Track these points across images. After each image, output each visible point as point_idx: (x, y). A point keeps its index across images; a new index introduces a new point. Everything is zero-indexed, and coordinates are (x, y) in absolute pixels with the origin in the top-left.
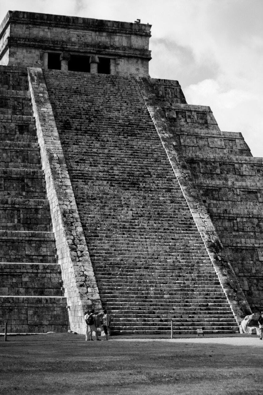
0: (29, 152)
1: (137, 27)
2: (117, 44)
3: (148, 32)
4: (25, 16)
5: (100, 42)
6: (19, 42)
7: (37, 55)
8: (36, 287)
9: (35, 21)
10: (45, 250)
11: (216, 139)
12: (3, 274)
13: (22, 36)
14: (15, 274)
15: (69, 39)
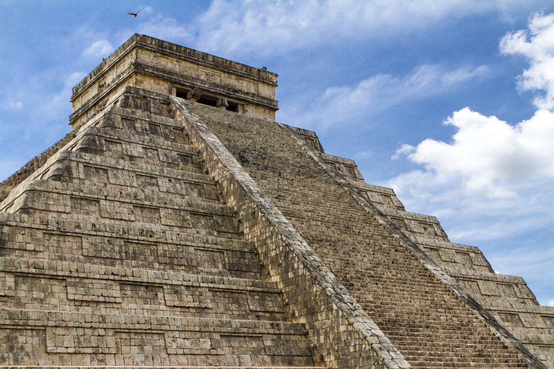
0: (205, 185)
1: (262, 74)
2: (246, 91)
3: (275, 81)
4: (154, 43)
5: (229, 84)
6: (146, 70)
7: (166, 89)
8: (283, 354)
9: (164, 50)
10: (270, 304)
11: (374, 193)
12: (239, 335)
13: (150, 64)
14: (254, 335)
15: (198, 76)
